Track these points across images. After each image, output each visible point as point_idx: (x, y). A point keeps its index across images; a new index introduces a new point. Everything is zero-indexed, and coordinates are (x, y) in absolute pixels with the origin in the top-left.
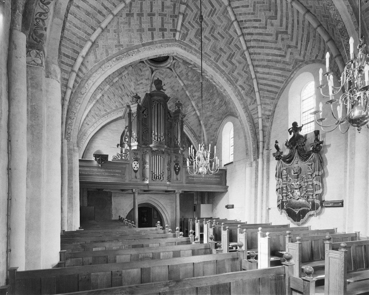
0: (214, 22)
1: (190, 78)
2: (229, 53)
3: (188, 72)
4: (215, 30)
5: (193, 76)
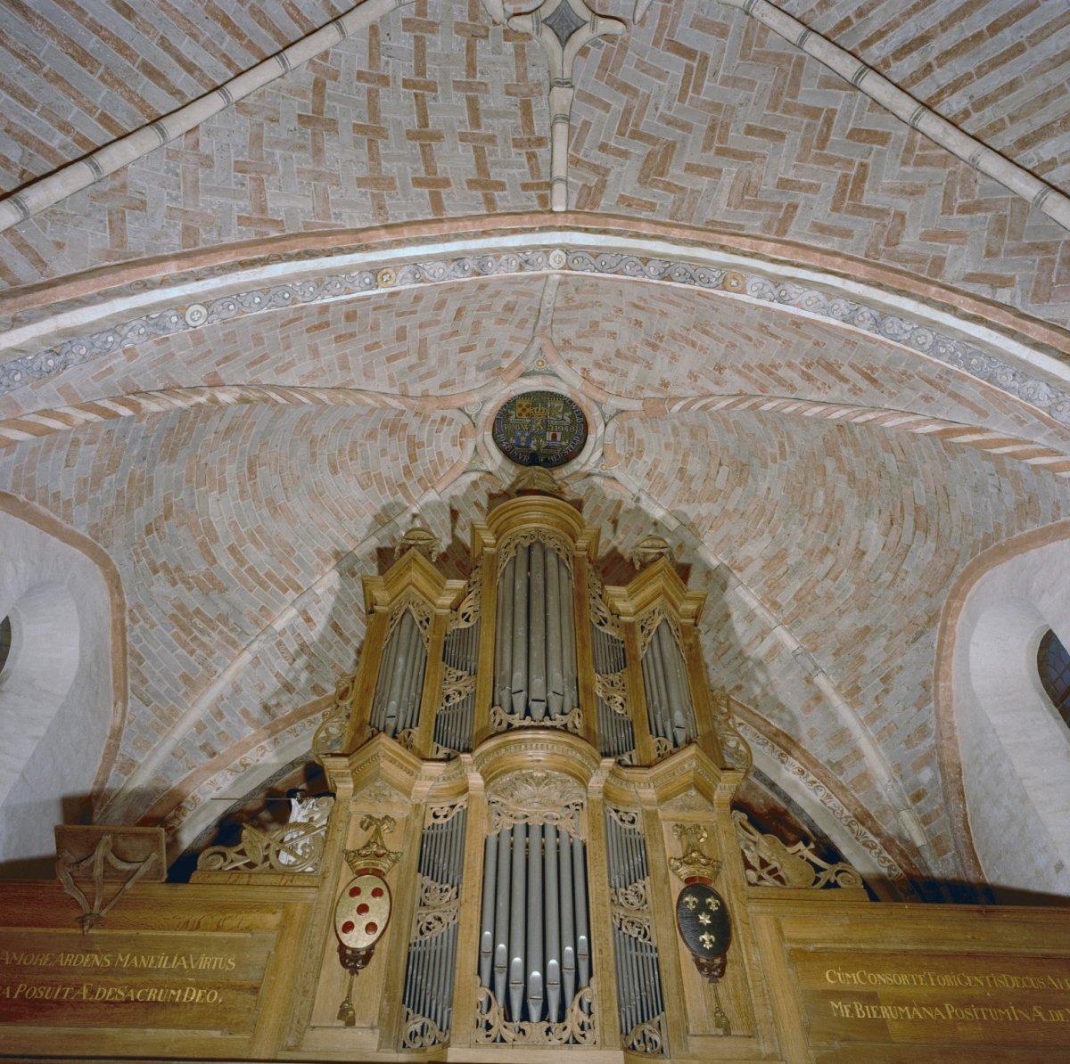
0: (711, 104)
1: (697, 485)
2: (836, 179)
3: (684, 461)
4: (726, 127)
5: (713, 471)
